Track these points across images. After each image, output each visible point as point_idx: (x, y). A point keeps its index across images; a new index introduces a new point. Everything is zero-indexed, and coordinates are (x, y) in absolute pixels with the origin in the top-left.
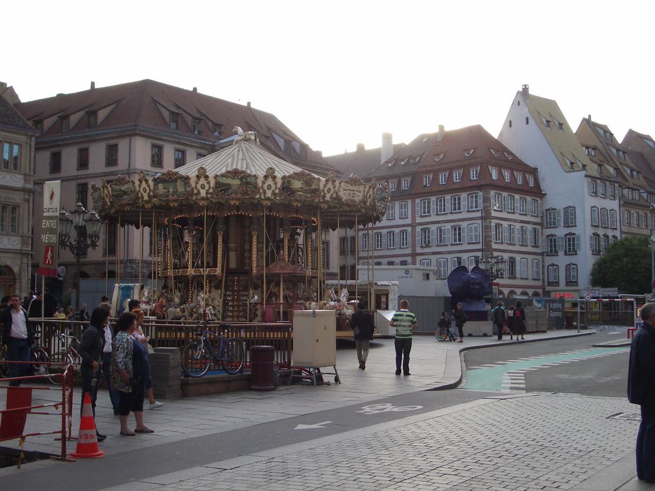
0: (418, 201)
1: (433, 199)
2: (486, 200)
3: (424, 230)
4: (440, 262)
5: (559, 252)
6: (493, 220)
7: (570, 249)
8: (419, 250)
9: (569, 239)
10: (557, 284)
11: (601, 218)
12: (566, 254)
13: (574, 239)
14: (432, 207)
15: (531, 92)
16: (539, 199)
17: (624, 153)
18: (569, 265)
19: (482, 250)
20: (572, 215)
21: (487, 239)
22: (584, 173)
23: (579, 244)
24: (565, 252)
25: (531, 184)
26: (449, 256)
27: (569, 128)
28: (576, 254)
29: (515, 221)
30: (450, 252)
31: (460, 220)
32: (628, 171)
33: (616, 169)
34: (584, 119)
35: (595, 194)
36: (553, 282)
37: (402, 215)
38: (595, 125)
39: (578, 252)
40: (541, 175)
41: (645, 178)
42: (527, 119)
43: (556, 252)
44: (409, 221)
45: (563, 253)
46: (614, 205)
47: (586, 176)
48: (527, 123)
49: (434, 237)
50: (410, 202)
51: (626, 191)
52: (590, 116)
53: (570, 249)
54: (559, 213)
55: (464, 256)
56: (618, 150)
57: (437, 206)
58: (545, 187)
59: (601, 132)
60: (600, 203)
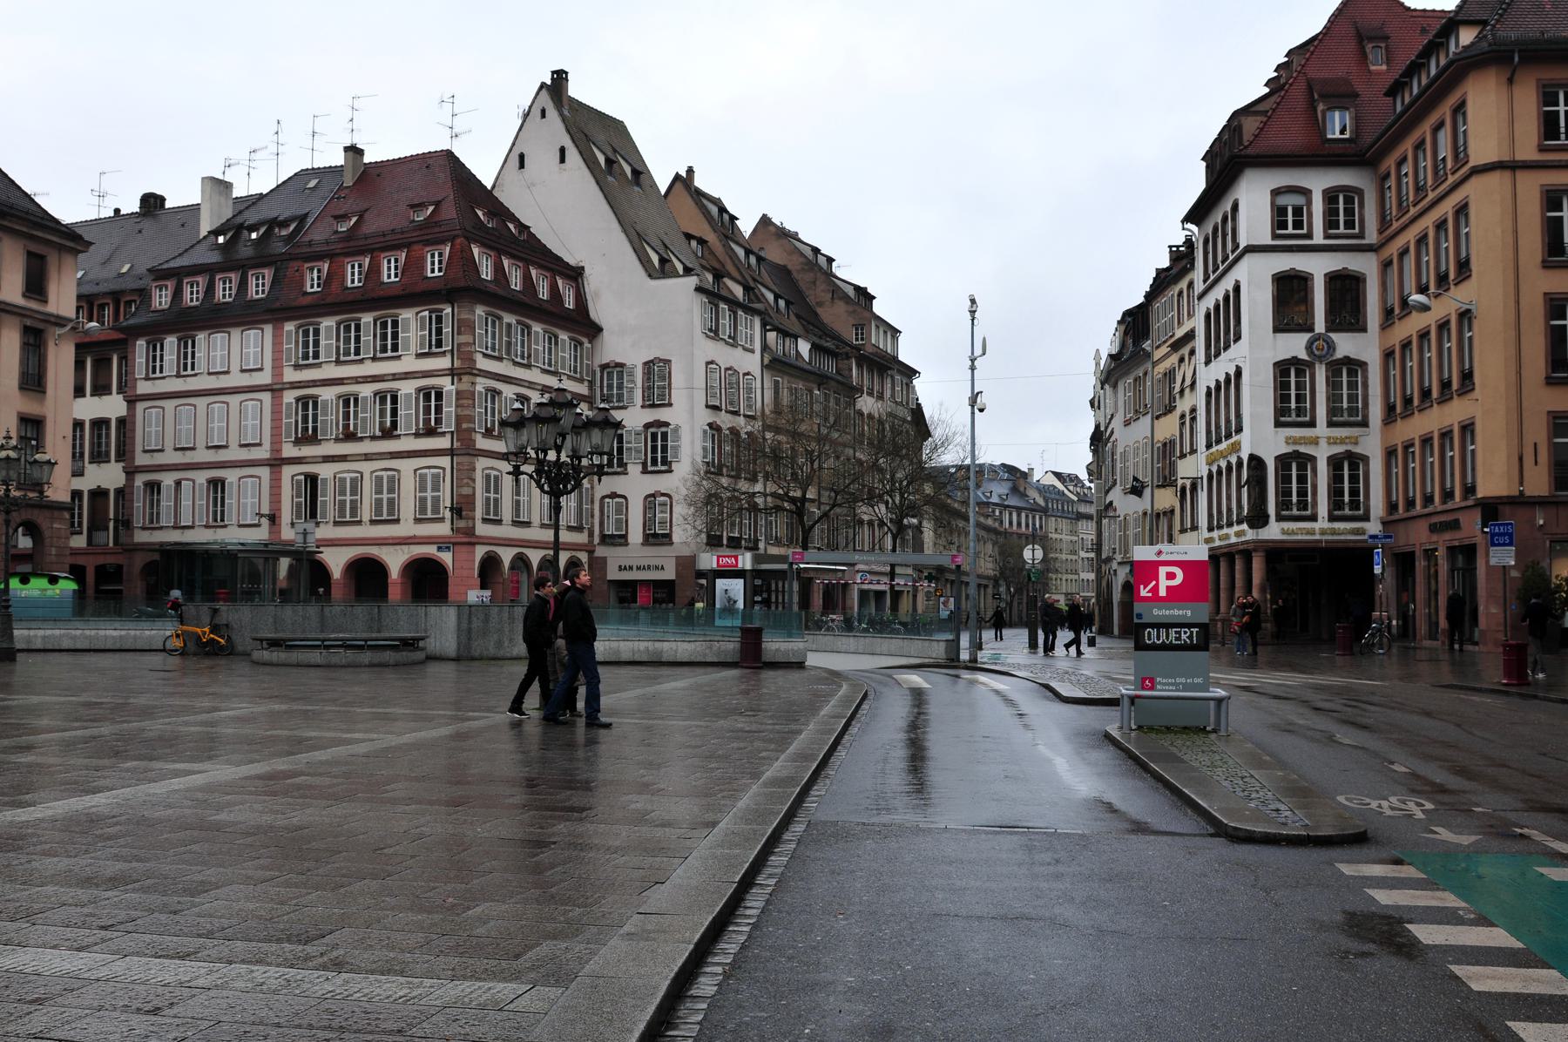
0: (289, 327)
1: (328, 323)
2: (464, 326)
3: (303, 401)
4: (343, 480)
5: (630, 467)
6: (479, 380)
7: (654, 462)
8: (289, 451)
9: (654, 436)
10: (621, 540)
11: (724, 390)
12: (645, 471)
13: (665, 436)
14: (322, 343)
15: (575, 90)
16: (585, 340)
17: (760, 259)
18: (653, 495)
19: (451, 452)
21: (464, 426)
22: (692, 281)
23: (676, 448)
24: (644, 464)
25: (570, 303)
26: (366, 467)
27: (654, 185)
28: (670, 471)
29: (531, 385)
30: (367, 457)
31: (396, 377)
32: (770, 297)
33: (747, 289)
34: (677, 177)
35: (714, 333)
36: (613, 536)
38: (699, 195)
39: (674, 466)
40: (592, 283)
41: (798, 317)
42: (562, 150)
43: (622, 464)
45: (640, 468)
46: (751, 363)
47: (699, 289)
48: (562, 160)
49: (331, 419)
50: (268, 329)
51: (772, 336)
52: (690, 171)
53: (654, 462)
54: (631, 374)
56: (748, 252)
57: (338, 340)
58: (598, 312)
59: (714, 210)
60: (727, 356)
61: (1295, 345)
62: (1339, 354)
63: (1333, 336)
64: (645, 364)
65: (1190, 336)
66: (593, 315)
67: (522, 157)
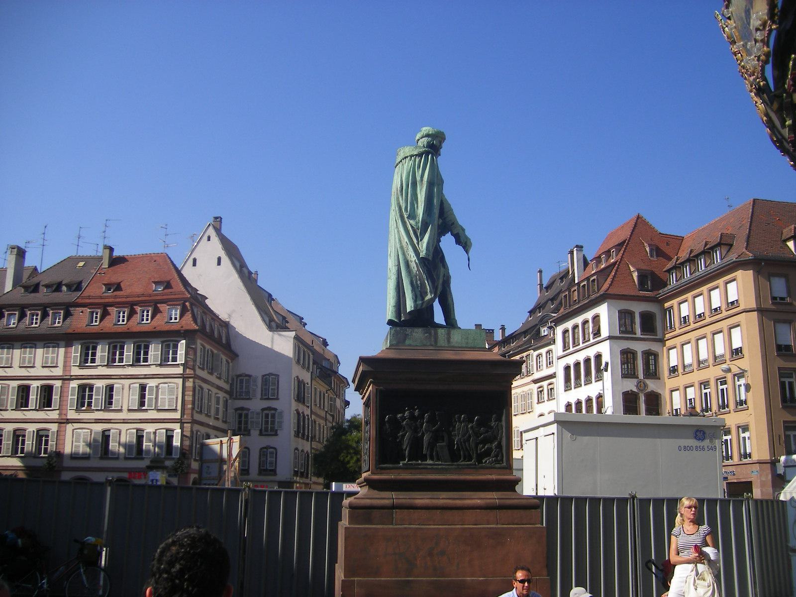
3: (82, 388)
4: (79, 434)
5: (252, 432)
7: (266, 430)
8: (72, 415)
12: (261, 434)
13: (273, 416)
20: (273, 384)
22: (293, 334)
23: (281, 423)
24: (261, 431)
28: (276, 435)
30: (125, 421)
31: (146, 377)
37: (47, 363)
39: (279, 432)
42: (219, 259)
44: (58, 372)
45: (258, 432)
48: (219, 263)
54: (255, 381)
55: (149, 428)
61: (630, 385)
62: (649, 390)
63: (648, 382)
64: (263, 376)
65: (553, 376)
66: (233, 347)
67: (195, 261)
